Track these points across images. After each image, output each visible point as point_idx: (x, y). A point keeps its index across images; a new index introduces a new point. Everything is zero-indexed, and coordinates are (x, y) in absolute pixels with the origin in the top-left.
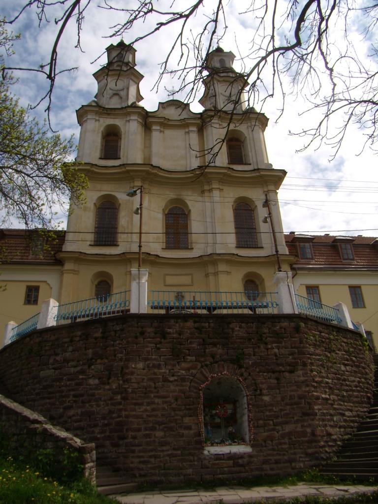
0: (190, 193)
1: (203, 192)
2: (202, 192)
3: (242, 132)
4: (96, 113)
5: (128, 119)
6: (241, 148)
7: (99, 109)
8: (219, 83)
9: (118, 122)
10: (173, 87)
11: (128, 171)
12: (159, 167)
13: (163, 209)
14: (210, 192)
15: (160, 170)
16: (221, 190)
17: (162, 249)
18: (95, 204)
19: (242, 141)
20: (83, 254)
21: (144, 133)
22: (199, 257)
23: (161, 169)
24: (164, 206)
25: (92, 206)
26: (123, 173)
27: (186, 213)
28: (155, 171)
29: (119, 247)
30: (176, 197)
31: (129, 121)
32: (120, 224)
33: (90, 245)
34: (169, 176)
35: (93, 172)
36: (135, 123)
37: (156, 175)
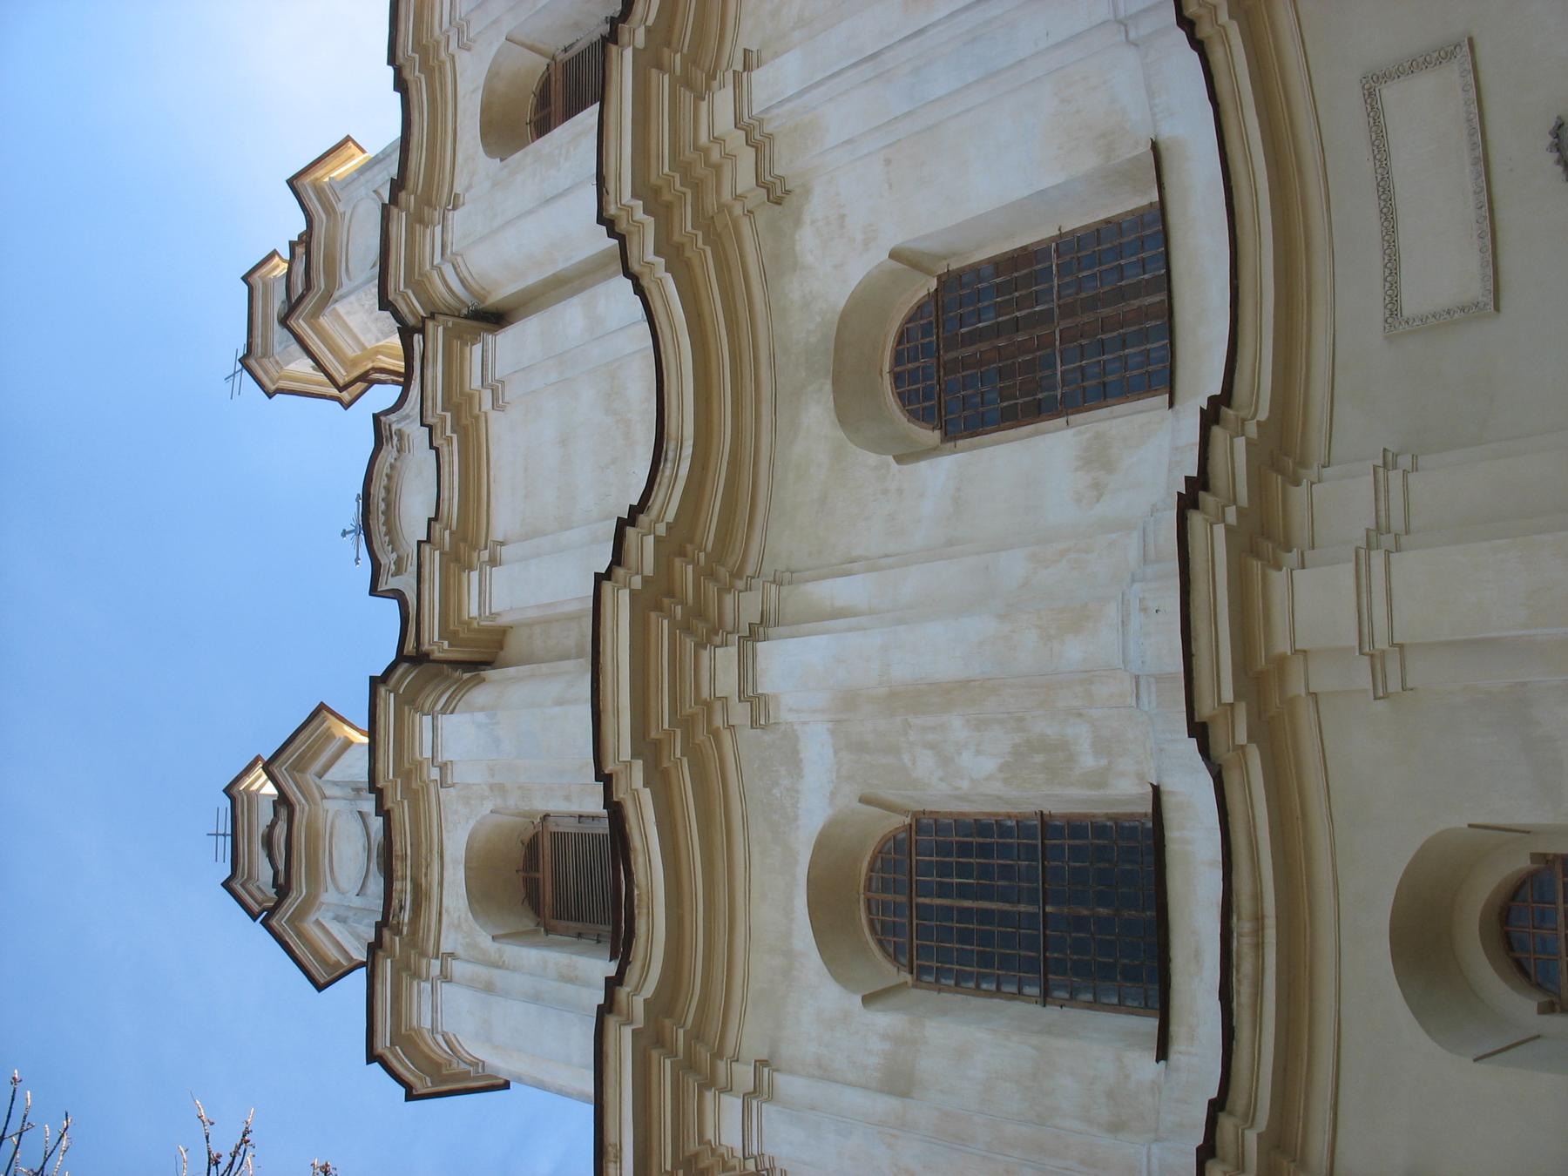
0: (794, 290)
1: (776, 193)
2: (778, 202)
3: (493, 75)
4: (407, 970)
5: (435, 774)
6: (580, 55)
7: (392, 955)
8: (337, 294)
9: (458, 830)
10: (344, 533)
11: (647, 746)
12: (622, 526)
13: (900, 459)
14: (770, 137)
15: (643, 518)
16: (750, 62)
17: (1171, 405)
18: (868, 1000)
19: (541, 64)
20: (1226, 1124)
21: (511, 671)
22: (1198, 45)
23: (636, 511)
24: (872, 458)
25: (884, 1020)
26: (658, 778)
27: (933, 284)
28: (644, 547)
29: (1173, 786)
30: (828, 386)
31: (443, 768)
32: (996, 788)
33: (1162, 1053)
34: (688, 451)
35: (665, 1004)
36: (447, 722)
37: (674, 545)
